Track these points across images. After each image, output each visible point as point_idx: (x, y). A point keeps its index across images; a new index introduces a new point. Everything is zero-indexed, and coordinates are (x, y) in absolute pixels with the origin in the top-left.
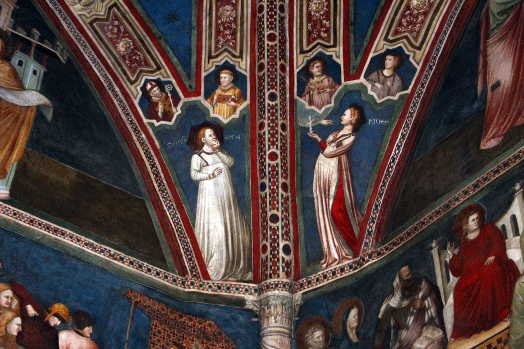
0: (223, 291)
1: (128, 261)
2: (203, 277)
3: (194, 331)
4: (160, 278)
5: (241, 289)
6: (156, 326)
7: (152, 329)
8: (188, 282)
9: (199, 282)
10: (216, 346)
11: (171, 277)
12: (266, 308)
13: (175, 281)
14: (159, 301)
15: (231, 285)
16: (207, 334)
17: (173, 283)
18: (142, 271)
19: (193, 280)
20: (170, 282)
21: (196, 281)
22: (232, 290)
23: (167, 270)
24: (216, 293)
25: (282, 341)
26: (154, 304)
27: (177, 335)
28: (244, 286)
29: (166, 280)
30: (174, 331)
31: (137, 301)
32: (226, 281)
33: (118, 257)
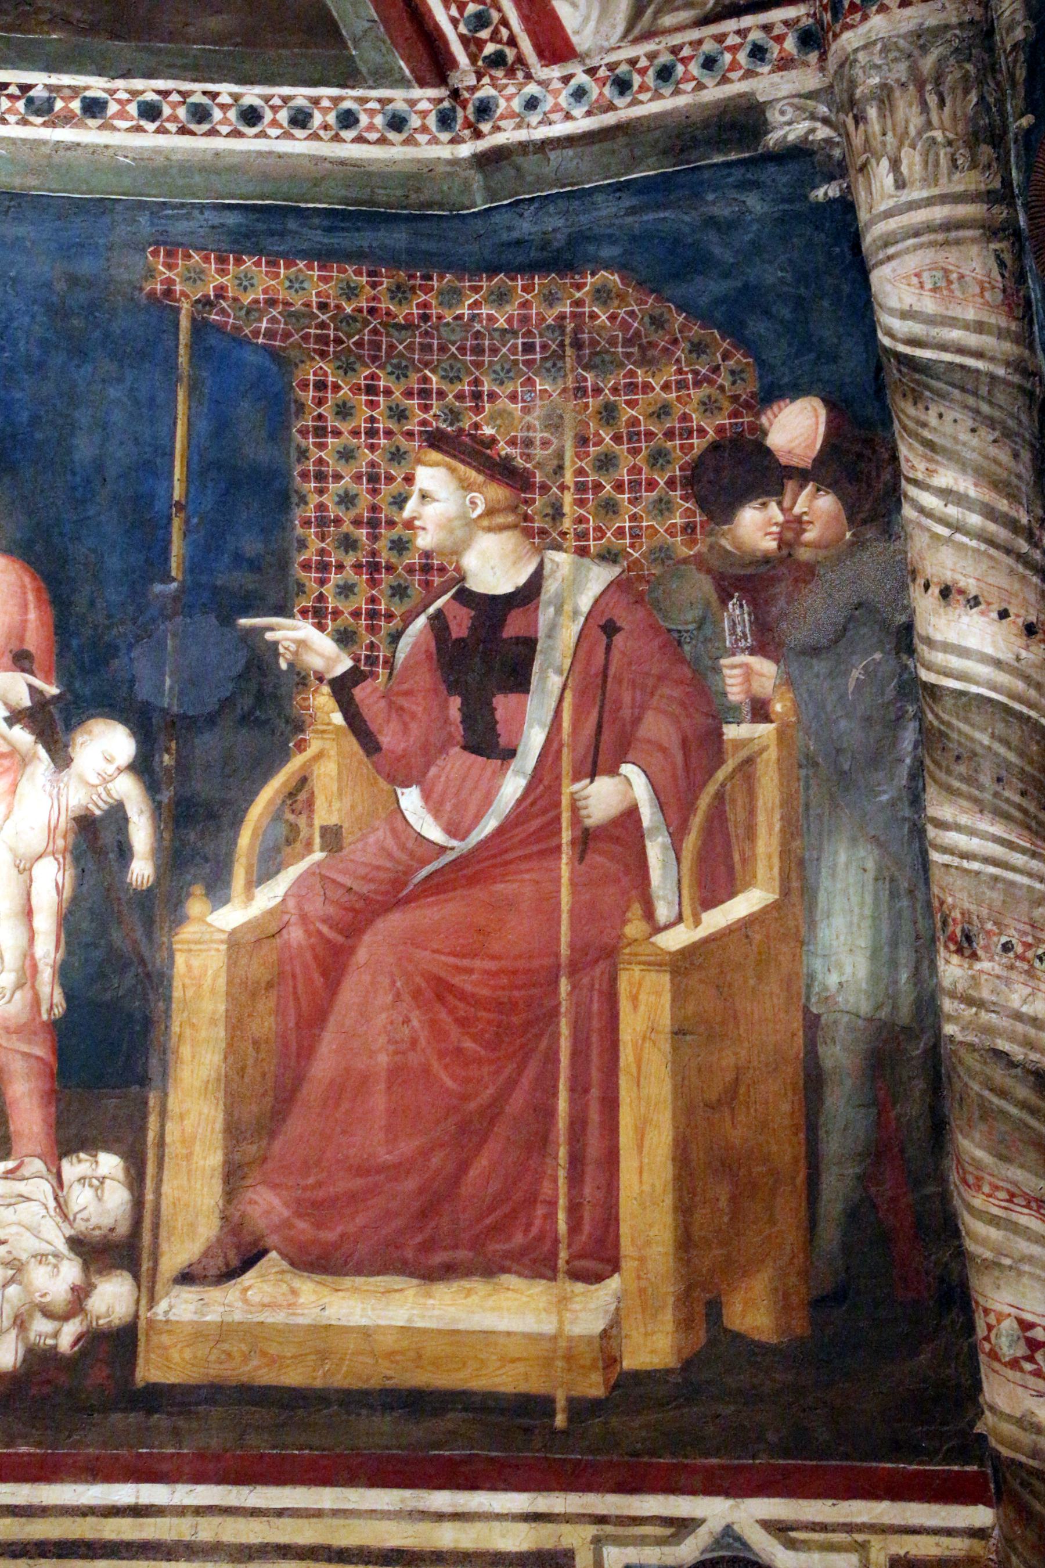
0: (642, 97)
1: (133, 109)
2: (541, 55)
3: (528, 348)
4: (315, 137)
5: (728, 57)
6: (321, 386)
7: (301, 407)
8: (464, 108)
9: (521, 86)
10: (647, 387)
11: (372, 113)
12: (850, 122)
13: (397, 123)
14: (324, 257)
15: (675, 50)
16: (594, 343)
17: (392, 136)
18: (213, 132)
19: (487, 91)
20: (373, 136)
21: (501, 89)
22: (687, 78)
23: (348, 77)
24: (609, 119)
25: (946, 272)
26: (295, 283)
27: (441, 394)
28: (738, 32)
29: (348, 134)
30: (426, 380)
31: (206, 296)
32: (648, 35)
33: (76, 105)
